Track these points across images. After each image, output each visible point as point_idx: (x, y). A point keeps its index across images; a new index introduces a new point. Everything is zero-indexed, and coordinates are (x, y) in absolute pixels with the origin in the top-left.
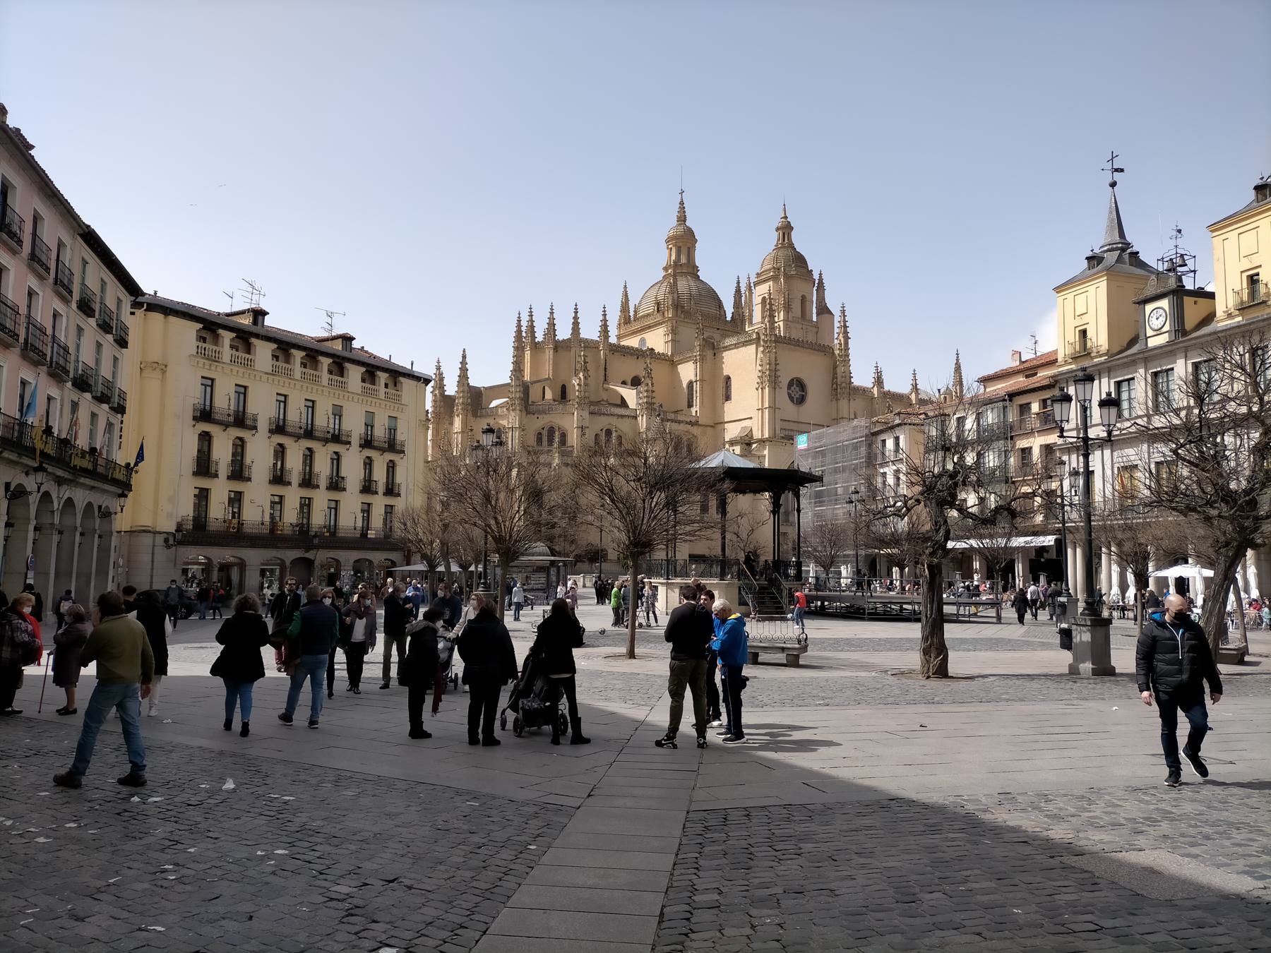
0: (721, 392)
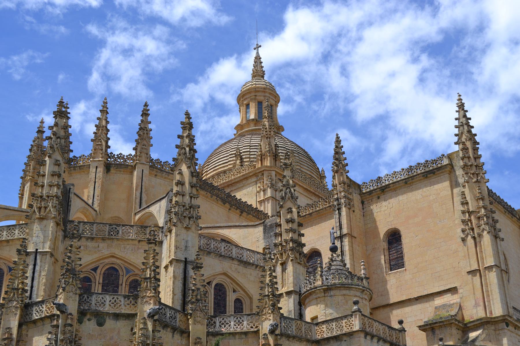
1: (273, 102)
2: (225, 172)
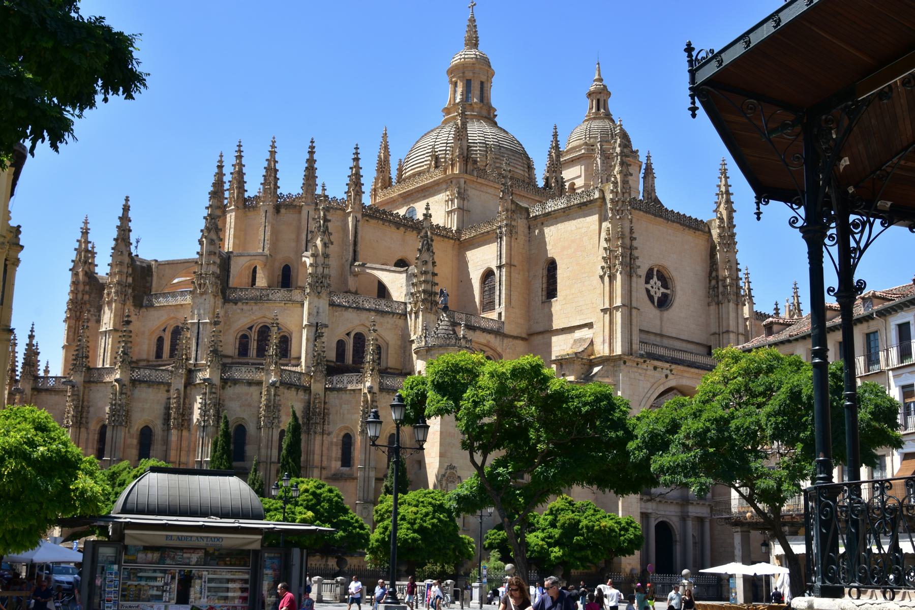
0: (539, 284)
1: (484, 78)
2: (419, 174)
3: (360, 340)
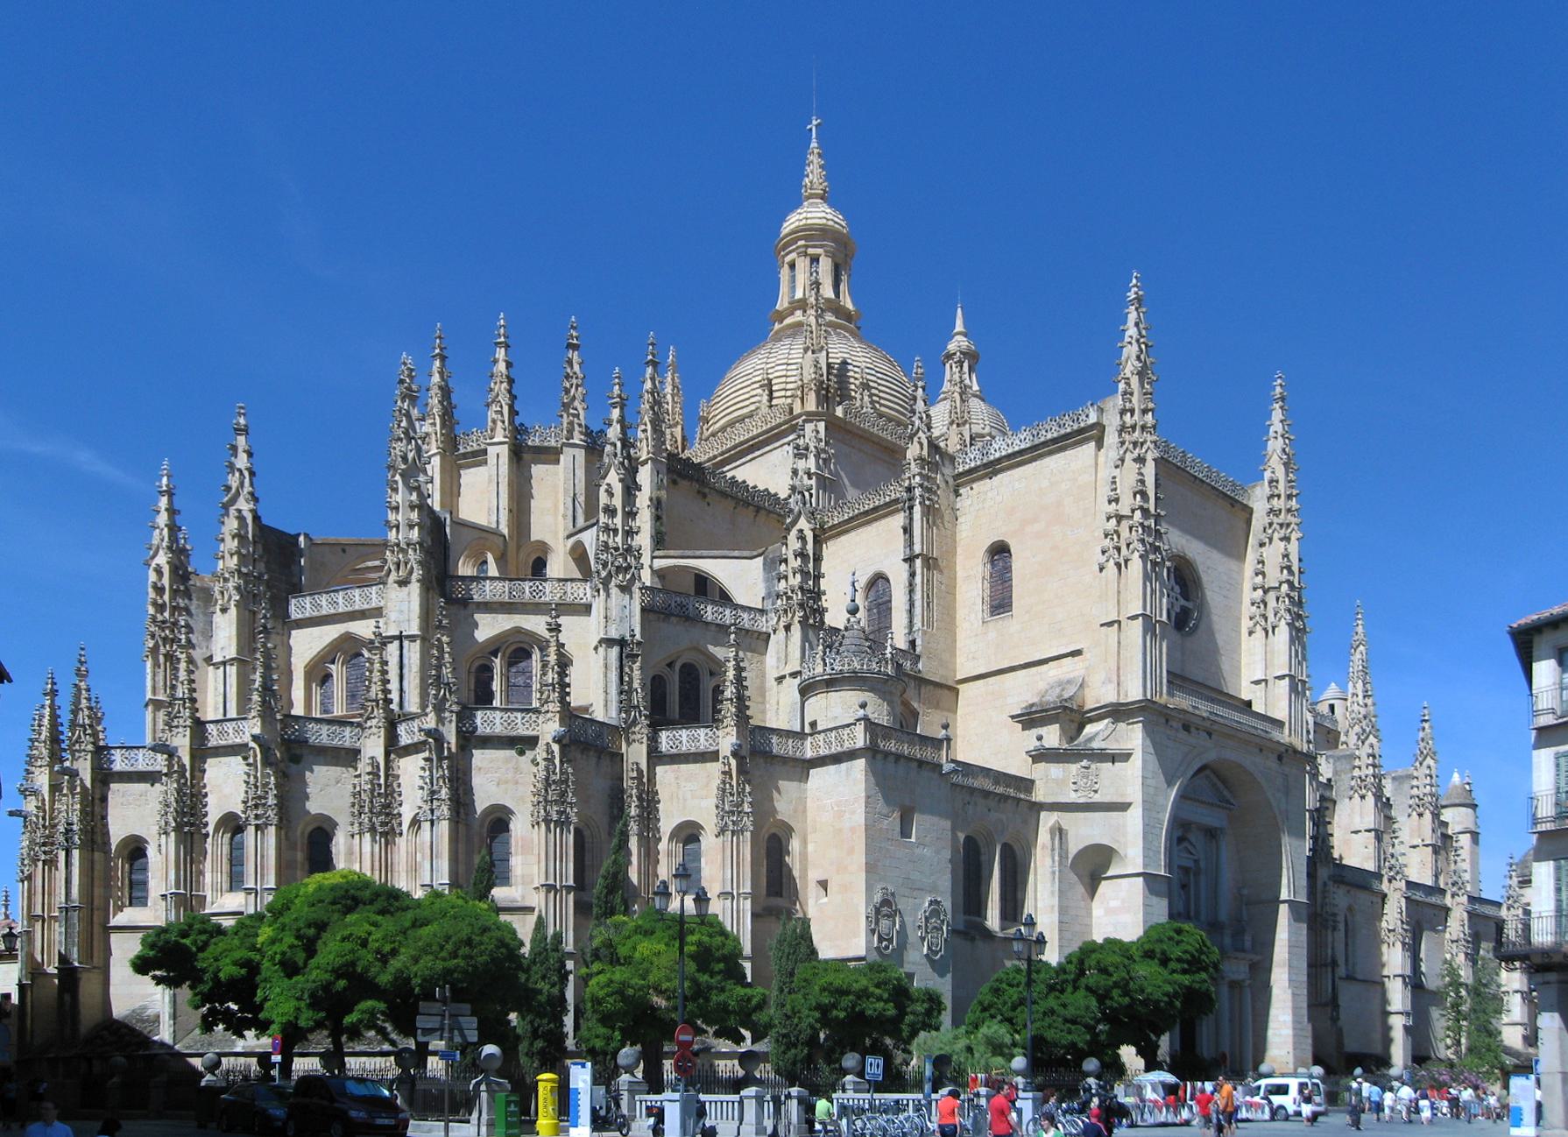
3: (690, 675)
